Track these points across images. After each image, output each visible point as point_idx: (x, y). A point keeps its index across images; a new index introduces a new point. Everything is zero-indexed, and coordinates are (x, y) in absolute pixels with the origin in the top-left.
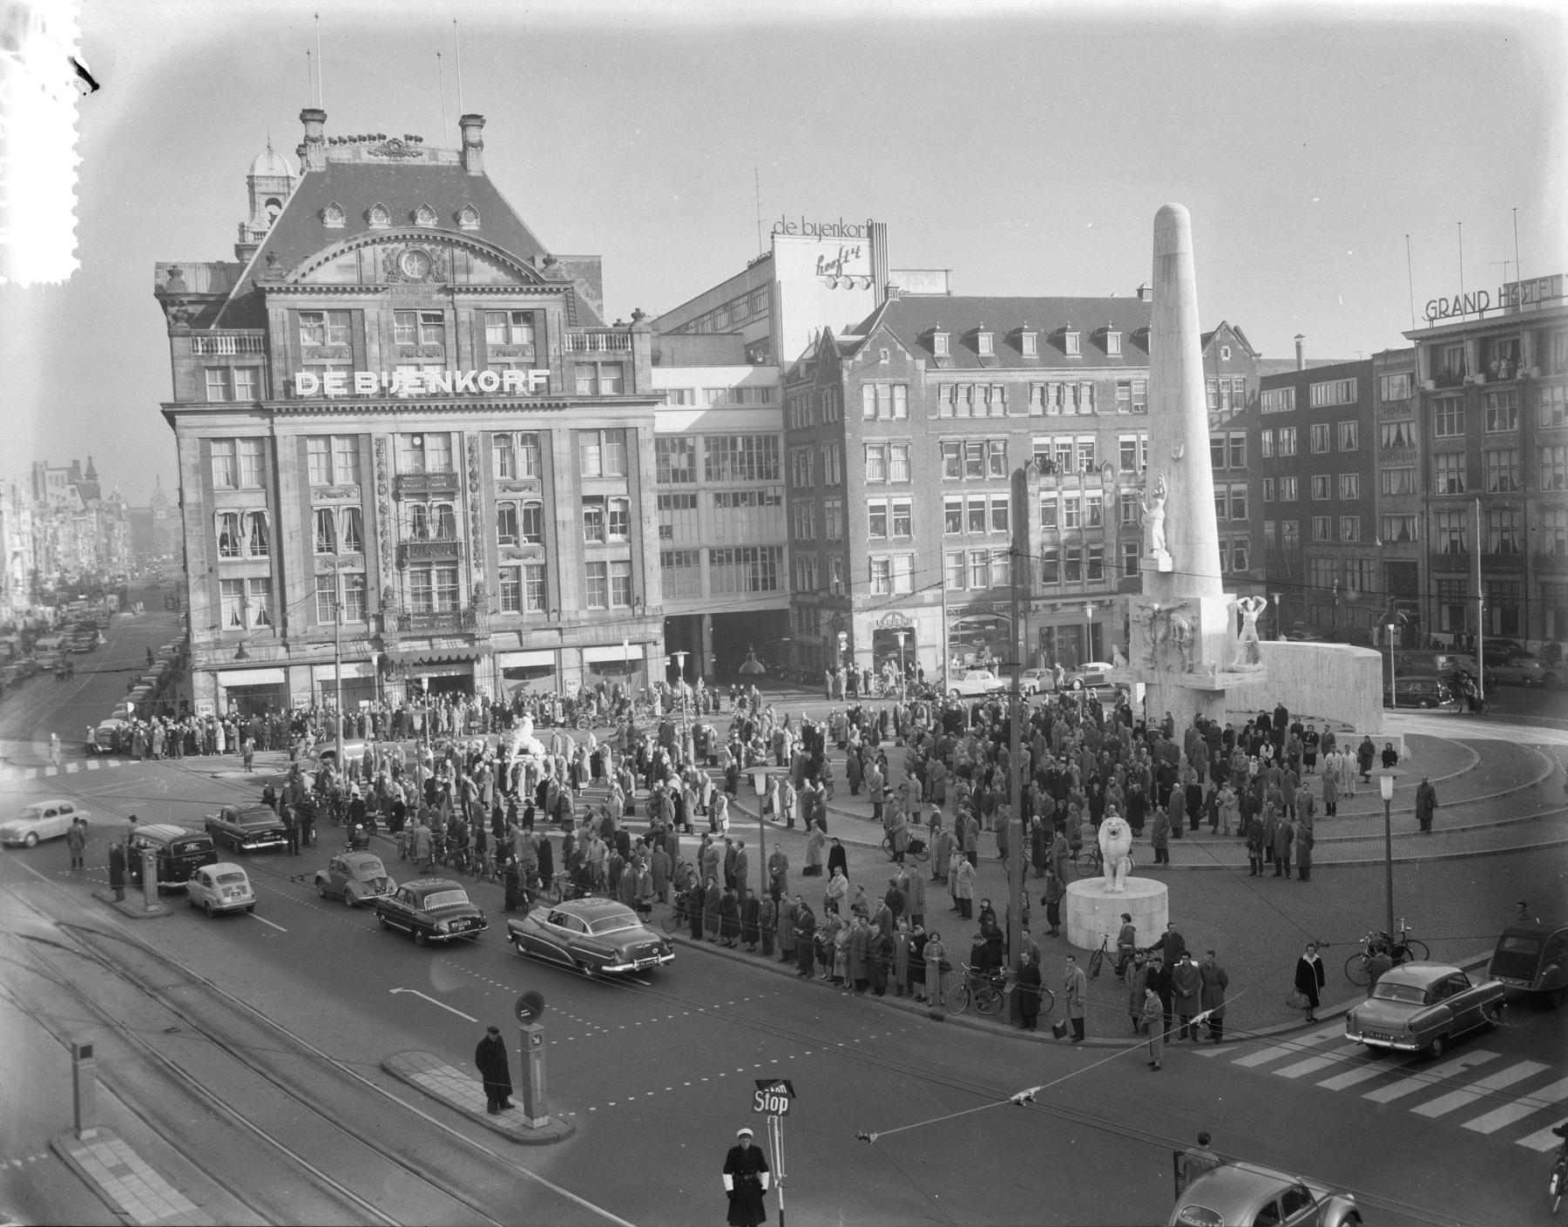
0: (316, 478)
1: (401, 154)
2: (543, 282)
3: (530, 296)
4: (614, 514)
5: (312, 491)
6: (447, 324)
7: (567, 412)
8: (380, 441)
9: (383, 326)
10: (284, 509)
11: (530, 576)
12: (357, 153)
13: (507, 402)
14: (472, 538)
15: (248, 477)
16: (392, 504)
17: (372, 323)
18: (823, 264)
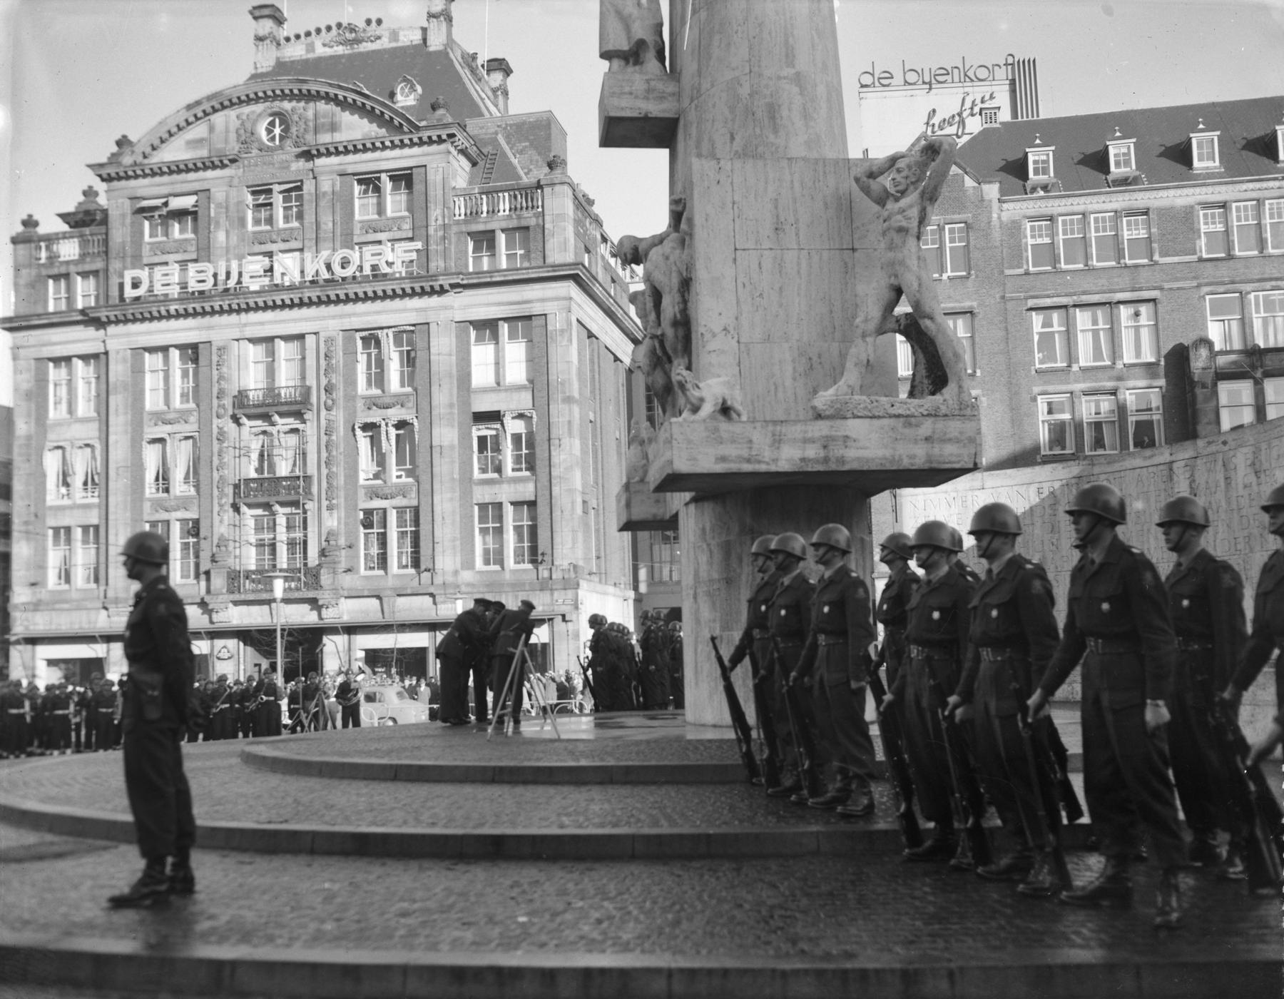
0: (153, 401)
1: (358, 41)
2: (418, 128)
3: (407, 151)
4: (517, 438)
5: (146, 418)
6: (306, 197)
7: (450, 299)
9: (232, 208)
10: (112, 438)
11: (401, 523)
12: (310, 48)
13: (378, 288)
14: (324, 471)
15: (85, 407)
16: (230, 427)
17: (219, 206)
18: (936, 120)
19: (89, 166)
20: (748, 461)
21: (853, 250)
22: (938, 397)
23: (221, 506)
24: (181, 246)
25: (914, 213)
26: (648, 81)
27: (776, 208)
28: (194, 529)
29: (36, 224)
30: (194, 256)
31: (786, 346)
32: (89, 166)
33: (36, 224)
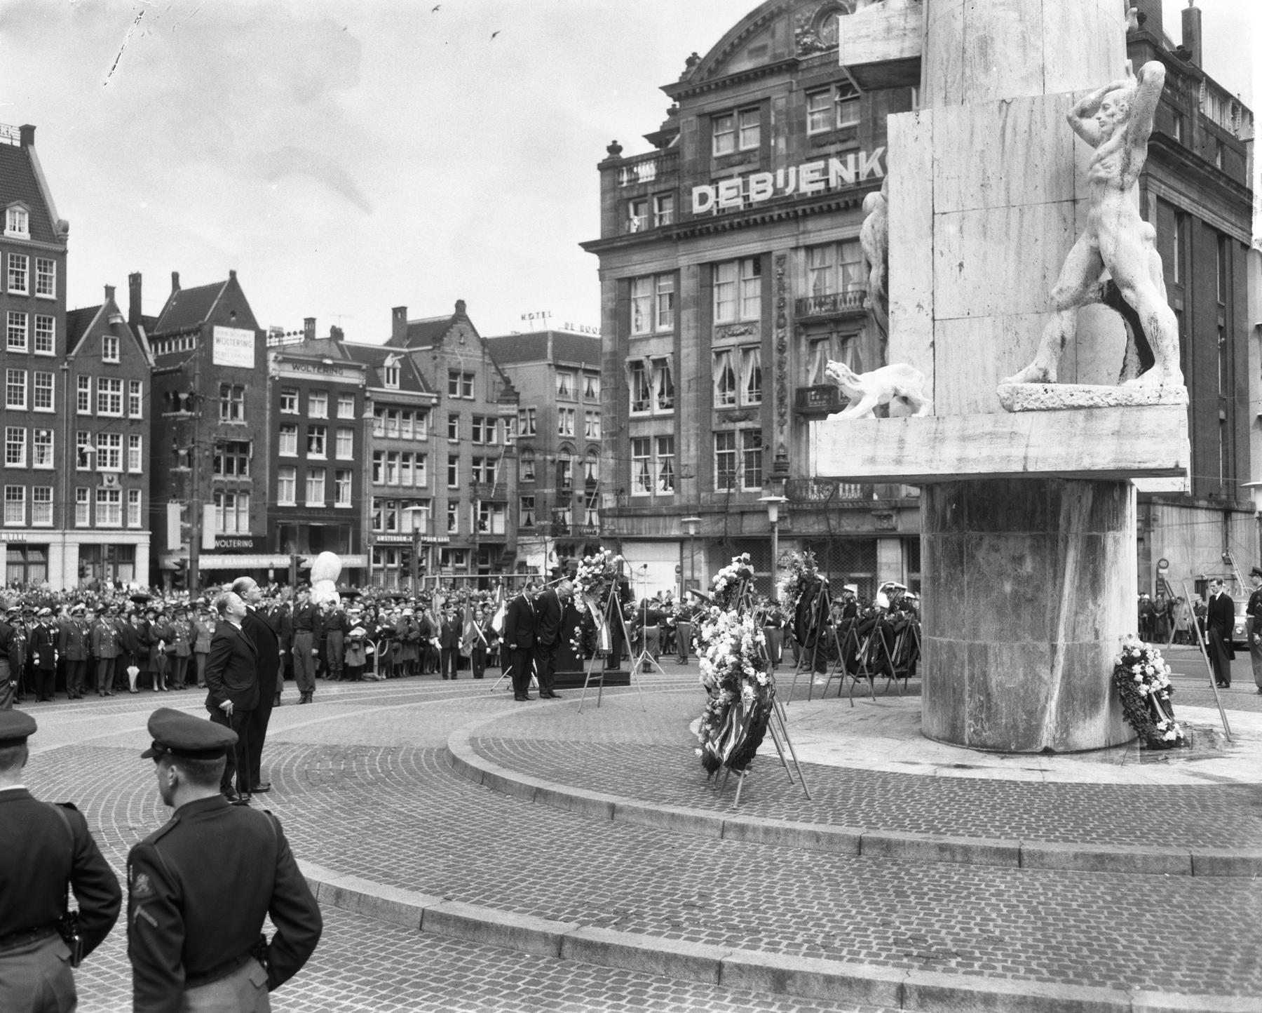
5: (714, 330)
8: (781, 259)
19: (663, 88)
20: (899, 462)
21: (1074, 201)
22: (1139, 381)
23: (782, 415)
24: (745, 157)
25: (1116, 161)
26: (887, 19)
27: (982, 161)
28: (754, 437)
29: (620, 149)
30: (757, 166)
31: (988, 320)
32: (663, 88)
33: (620, 149)
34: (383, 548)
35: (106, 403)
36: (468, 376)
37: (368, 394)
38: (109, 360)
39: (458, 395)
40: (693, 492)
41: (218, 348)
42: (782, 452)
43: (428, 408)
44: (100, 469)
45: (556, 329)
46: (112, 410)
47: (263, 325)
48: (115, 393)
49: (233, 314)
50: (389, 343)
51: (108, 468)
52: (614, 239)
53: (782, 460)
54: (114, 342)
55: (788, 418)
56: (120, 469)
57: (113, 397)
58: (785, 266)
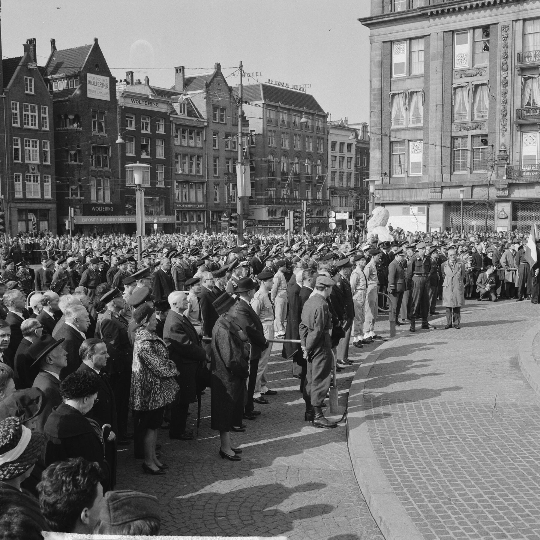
8: (506, 28)
23: (504, 126)
34: (181, 211)
35: (28, 120)
36: (223, 110)
37: (171, 119)
38: (28, 92)
39: (217, 121)
40: (438, 174)
41: (89, 87)
42: (503, 148)
43: (203, 128)
44: (26, 162)
45: (264, 83)
46: (32, 125)
47: (113, 75)
48: (33, 114)
49: (97, 66)
50: (174, 88)
51: (31, 162)
52: (378, 17)
53: (502, 153)
54: (31, 81)
55: (508, 127)
56: (38, 162)
57: (32, 116)
58: (510, 32)
